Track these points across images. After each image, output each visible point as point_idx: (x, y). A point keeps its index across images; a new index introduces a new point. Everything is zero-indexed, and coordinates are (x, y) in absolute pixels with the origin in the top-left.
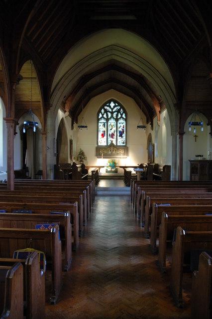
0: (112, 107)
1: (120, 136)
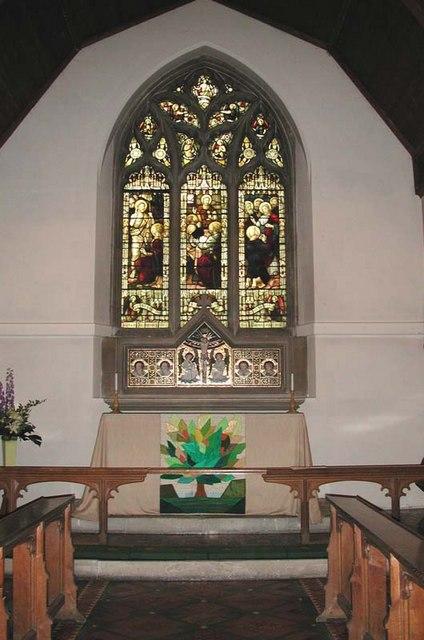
0: (204, 102)
1: (251, 274)
